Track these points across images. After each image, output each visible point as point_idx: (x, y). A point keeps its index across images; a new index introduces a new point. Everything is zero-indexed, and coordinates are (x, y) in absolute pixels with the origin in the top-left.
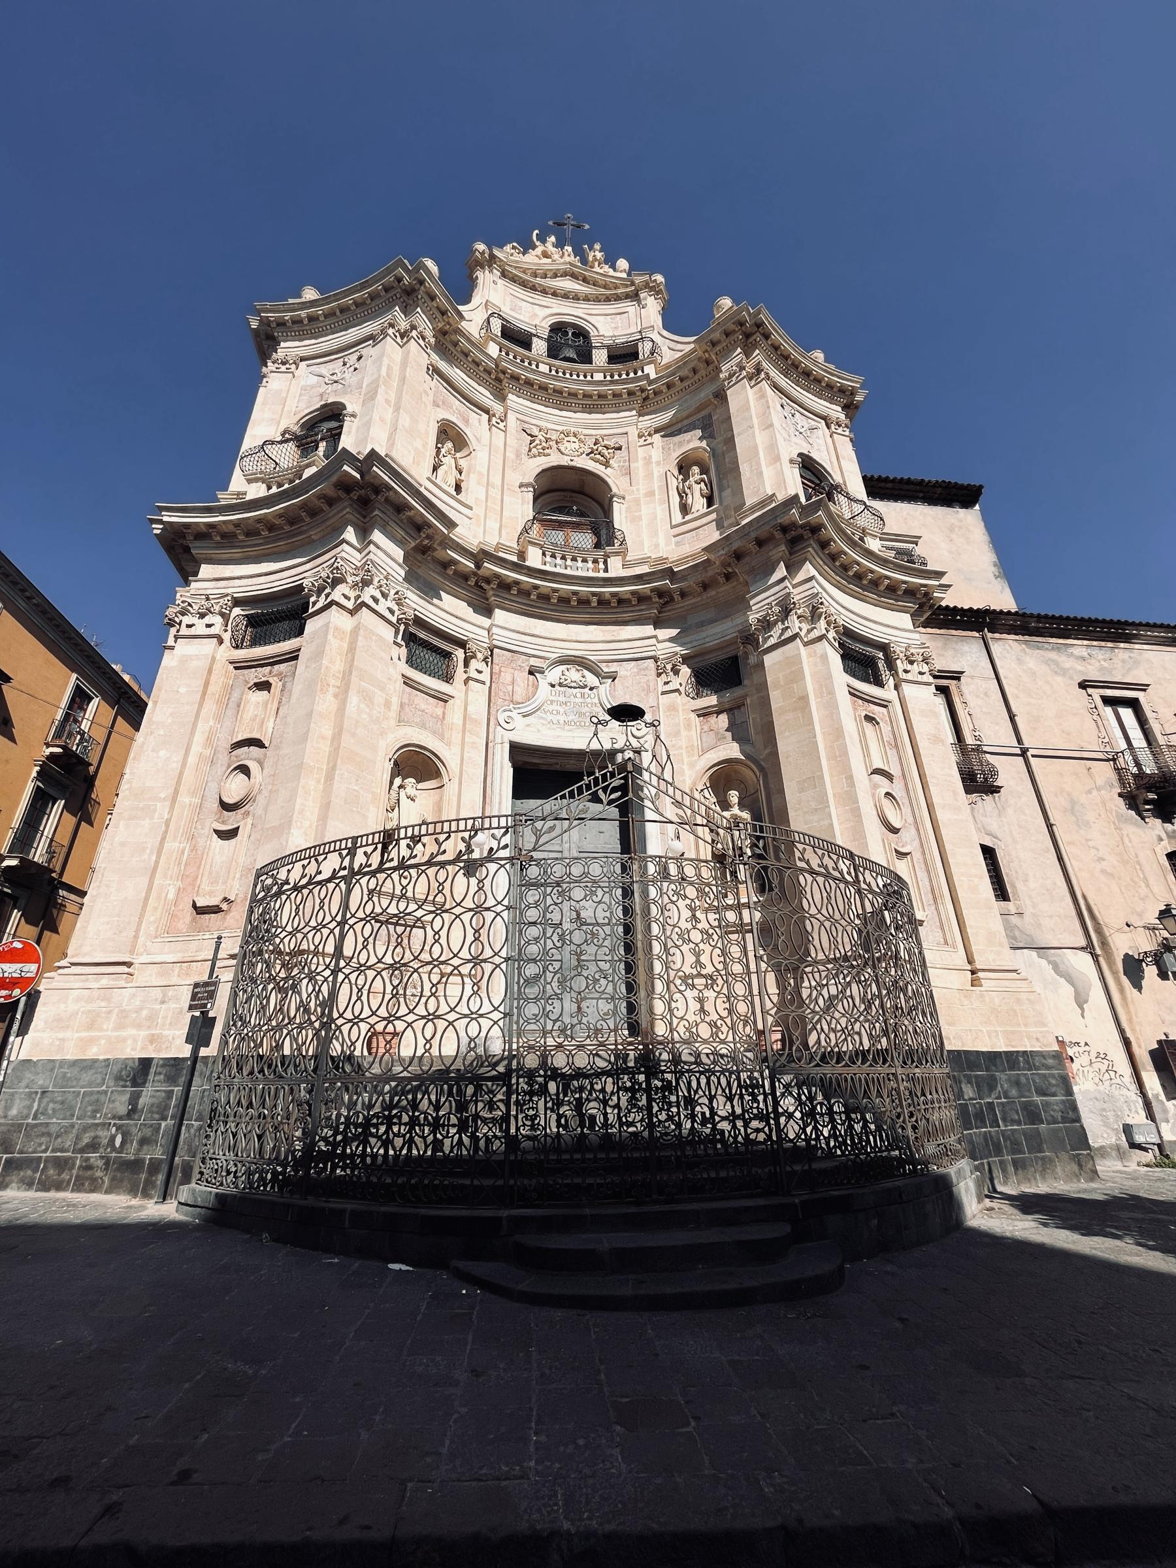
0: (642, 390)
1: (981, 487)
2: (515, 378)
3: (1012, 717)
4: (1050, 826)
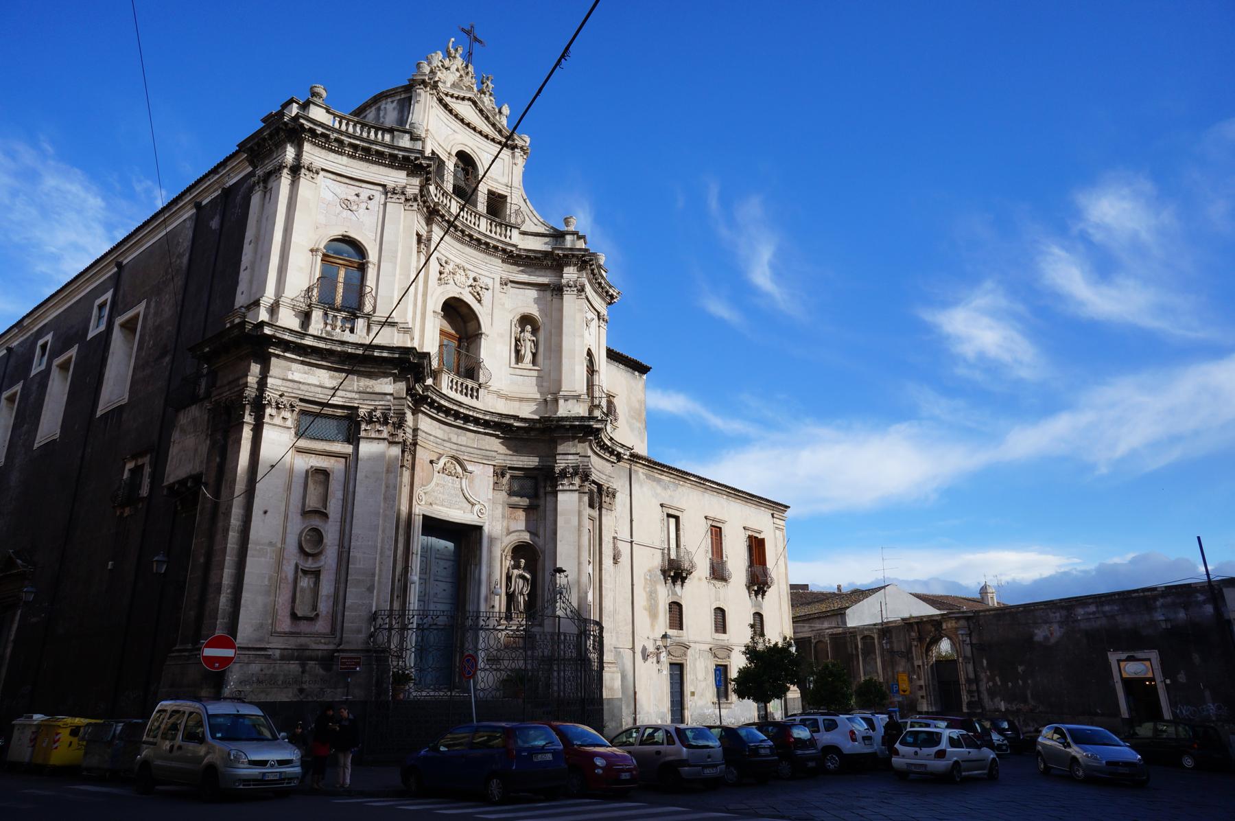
0: (511, 251)
1: (651, 368)
2: (443, 216)
3: (631, 521)
4: (632, 585)
